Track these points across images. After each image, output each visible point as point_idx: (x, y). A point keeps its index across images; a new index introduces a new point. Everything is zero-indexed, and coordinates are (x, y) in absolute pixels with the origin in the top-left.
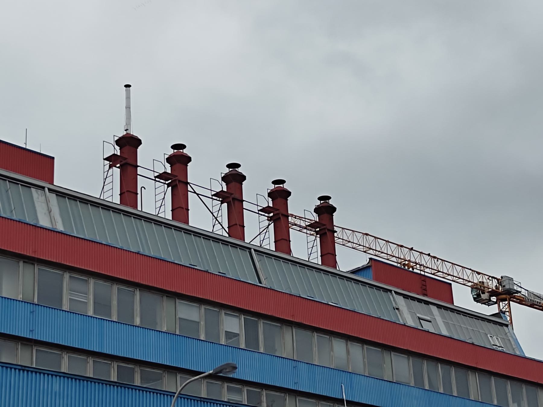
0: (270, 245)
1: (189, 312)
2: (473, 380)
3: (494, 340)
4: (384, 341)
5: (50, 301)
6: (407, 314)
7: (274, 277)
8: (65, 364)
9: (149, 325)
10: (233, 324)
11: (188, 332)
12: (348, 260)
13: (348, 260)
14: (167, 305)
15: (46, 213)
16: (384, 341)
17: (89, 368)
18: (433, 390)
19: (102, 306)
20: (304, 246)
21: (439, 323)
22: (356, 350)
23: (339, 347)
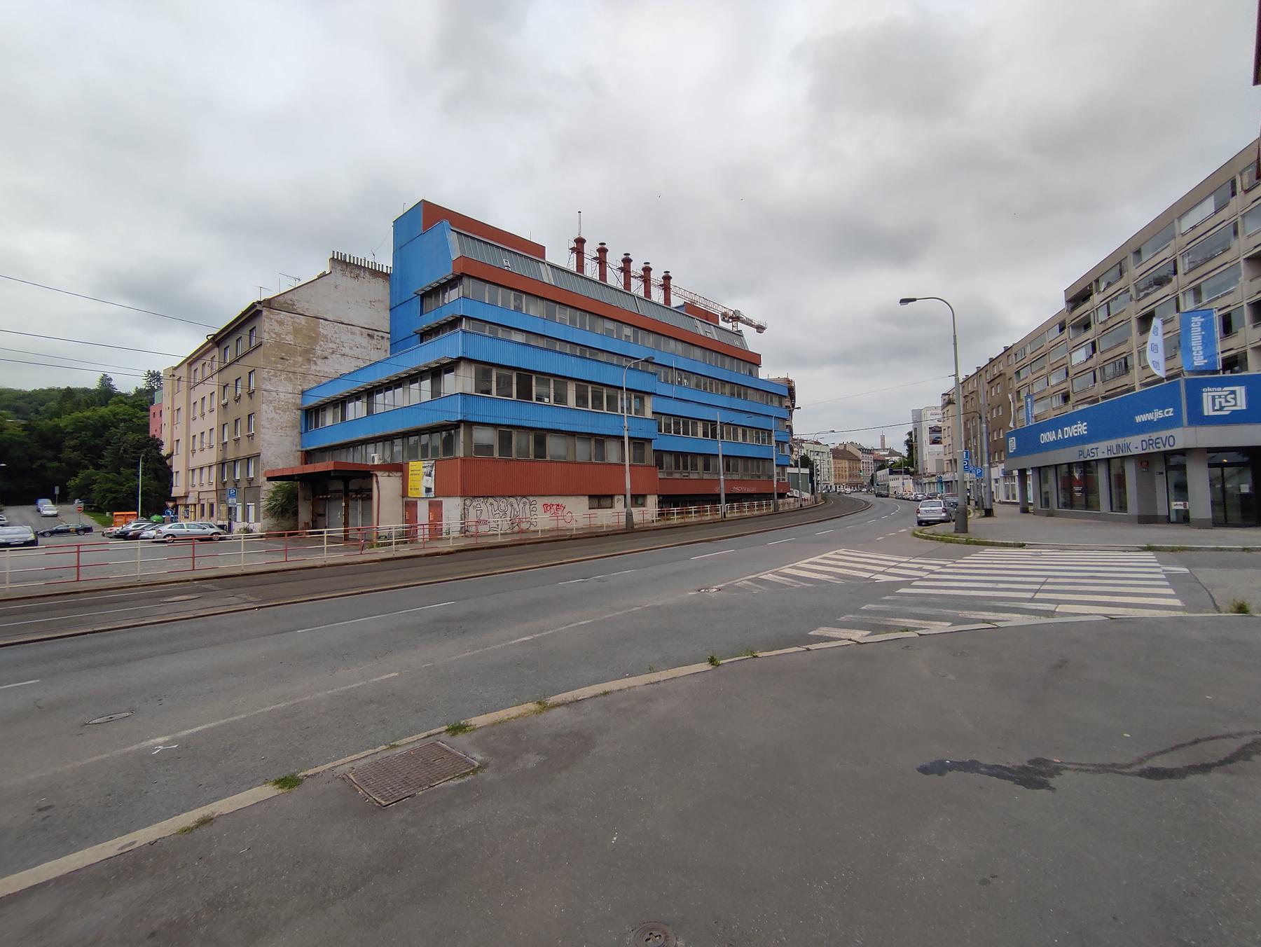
0: (642, 294)
1: (610, 325)
2: (727, 360)
3: (737, 344)
4: (690, 341)
5: (551, 317)
6: (701, 329)
7: (644, 310)
8: (558, 347)
9: (592, 330)
10: (628, 331)
11: (609, 333)
12: (676, 301)
13: (676, 301)
14: (600, 322)
15: (547, 277)
16: (690, 341)
17: (568, 349)
18: (710, 364)
19: (573, 321)
20: (657, 295)
21: (714, 334)
22: (680, 345)
23: (672, 343)
